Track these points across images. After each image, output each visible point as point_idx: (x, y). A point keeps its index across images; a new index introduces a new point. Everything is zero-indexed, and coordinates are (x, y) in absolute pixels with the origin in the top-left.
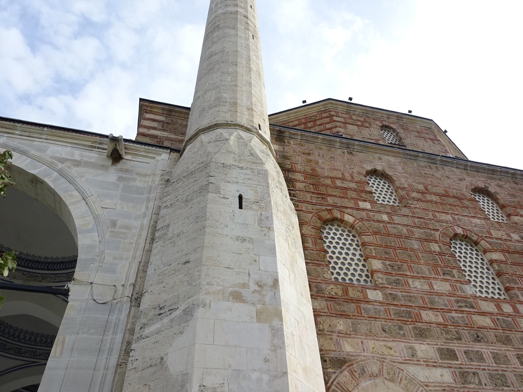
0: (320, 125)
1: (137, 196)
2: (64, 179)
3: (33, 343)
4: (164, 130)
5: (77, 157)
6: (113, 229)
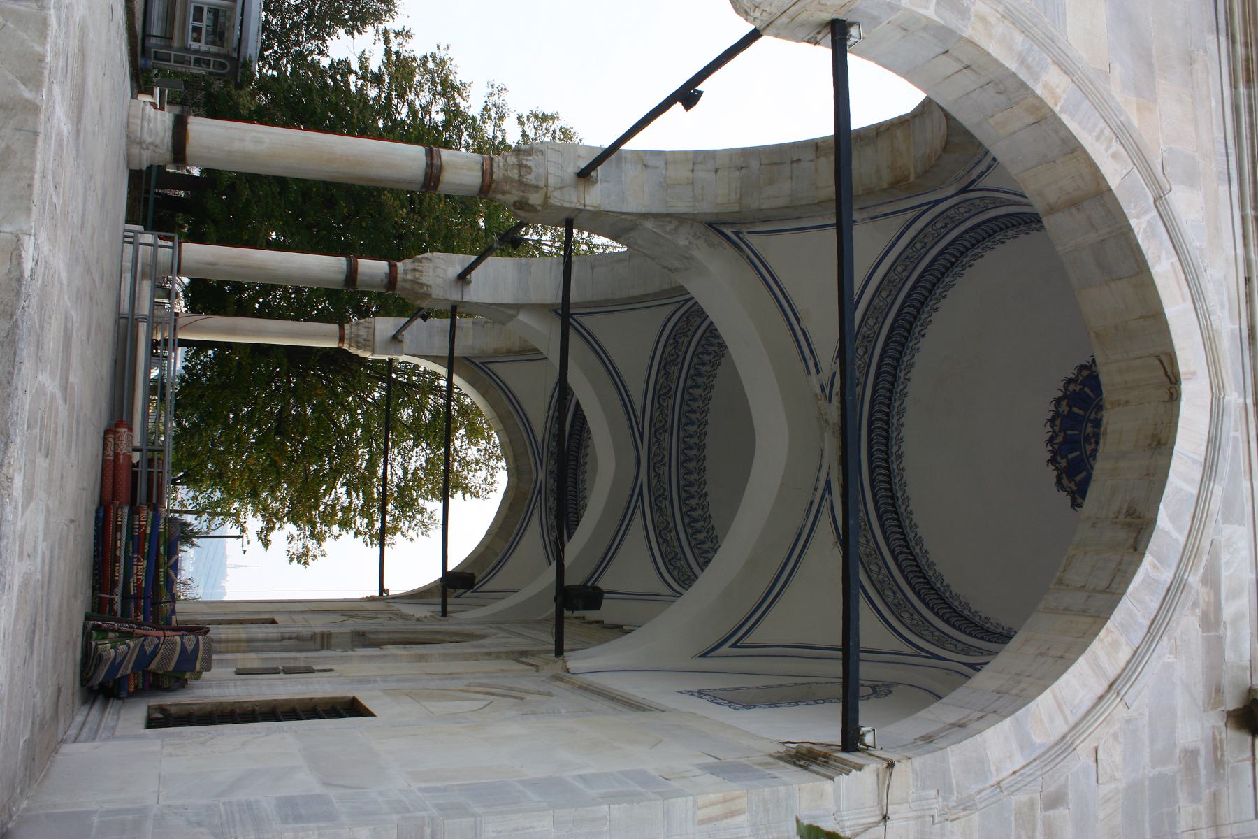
1: (1147, 826)
2: (1156, 605)
3: (683, 420)
5: (1228, 611)
6: (1039, 805)
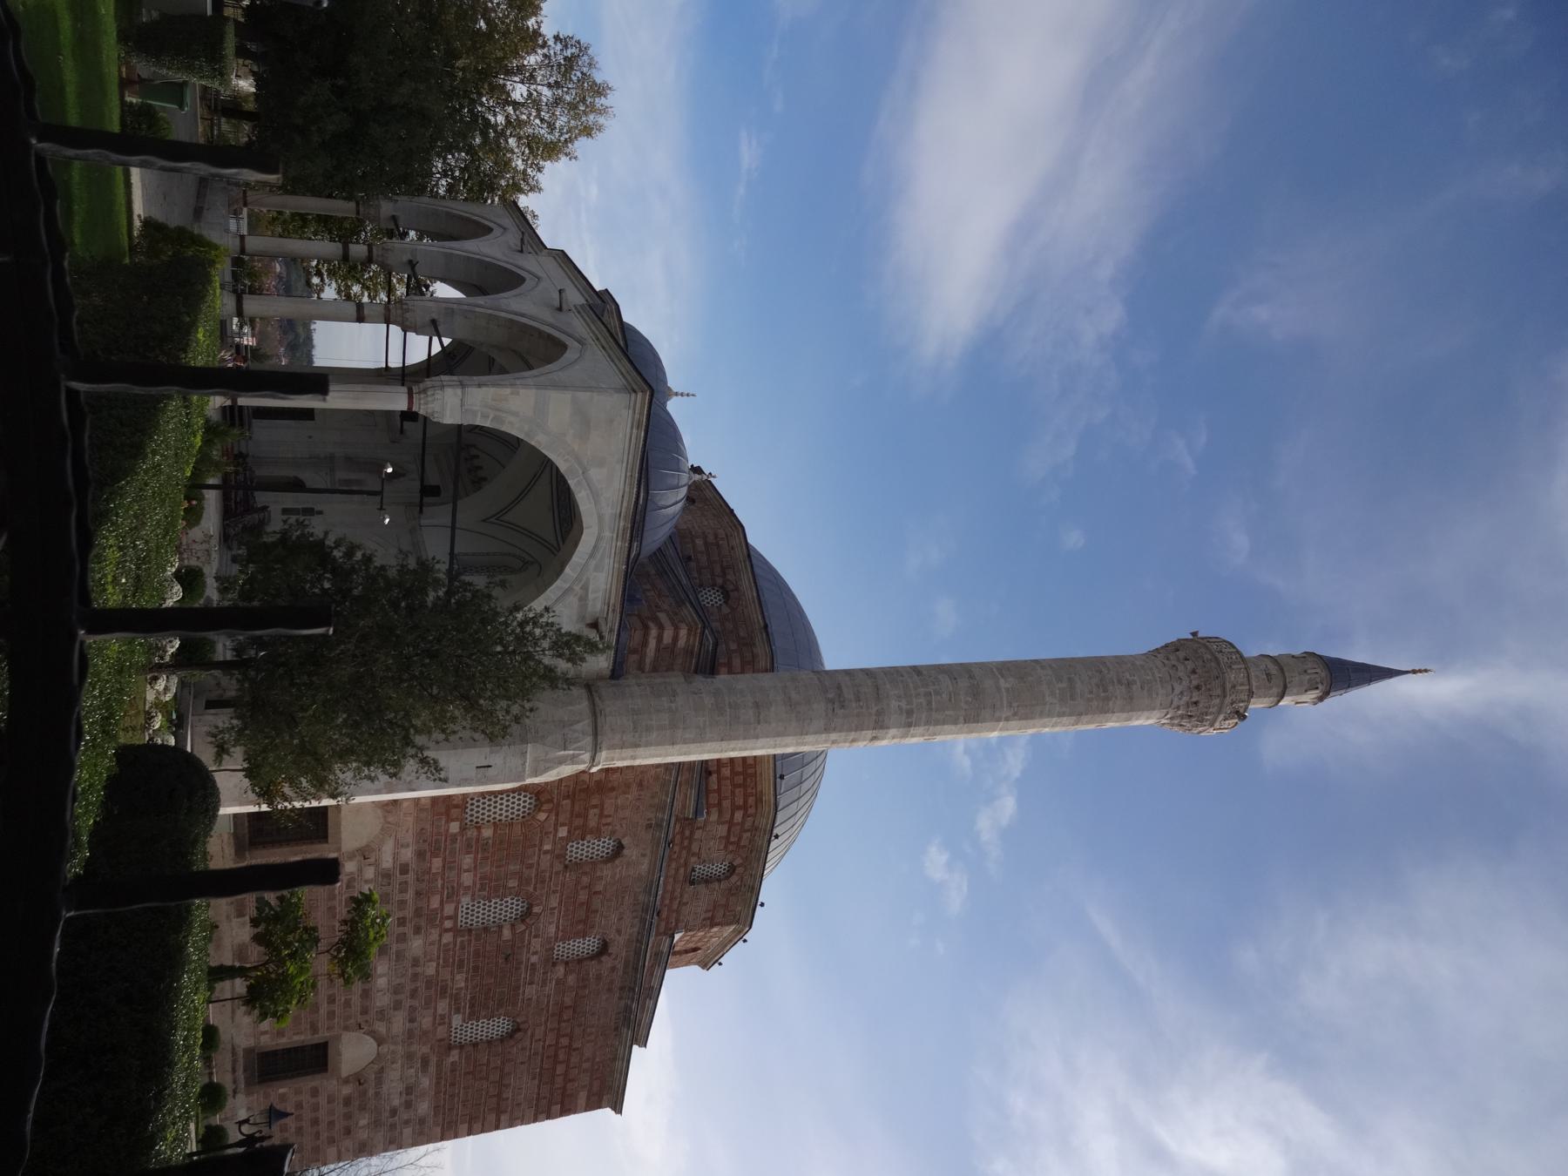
0: (733, 793)
4: (658, 650)
